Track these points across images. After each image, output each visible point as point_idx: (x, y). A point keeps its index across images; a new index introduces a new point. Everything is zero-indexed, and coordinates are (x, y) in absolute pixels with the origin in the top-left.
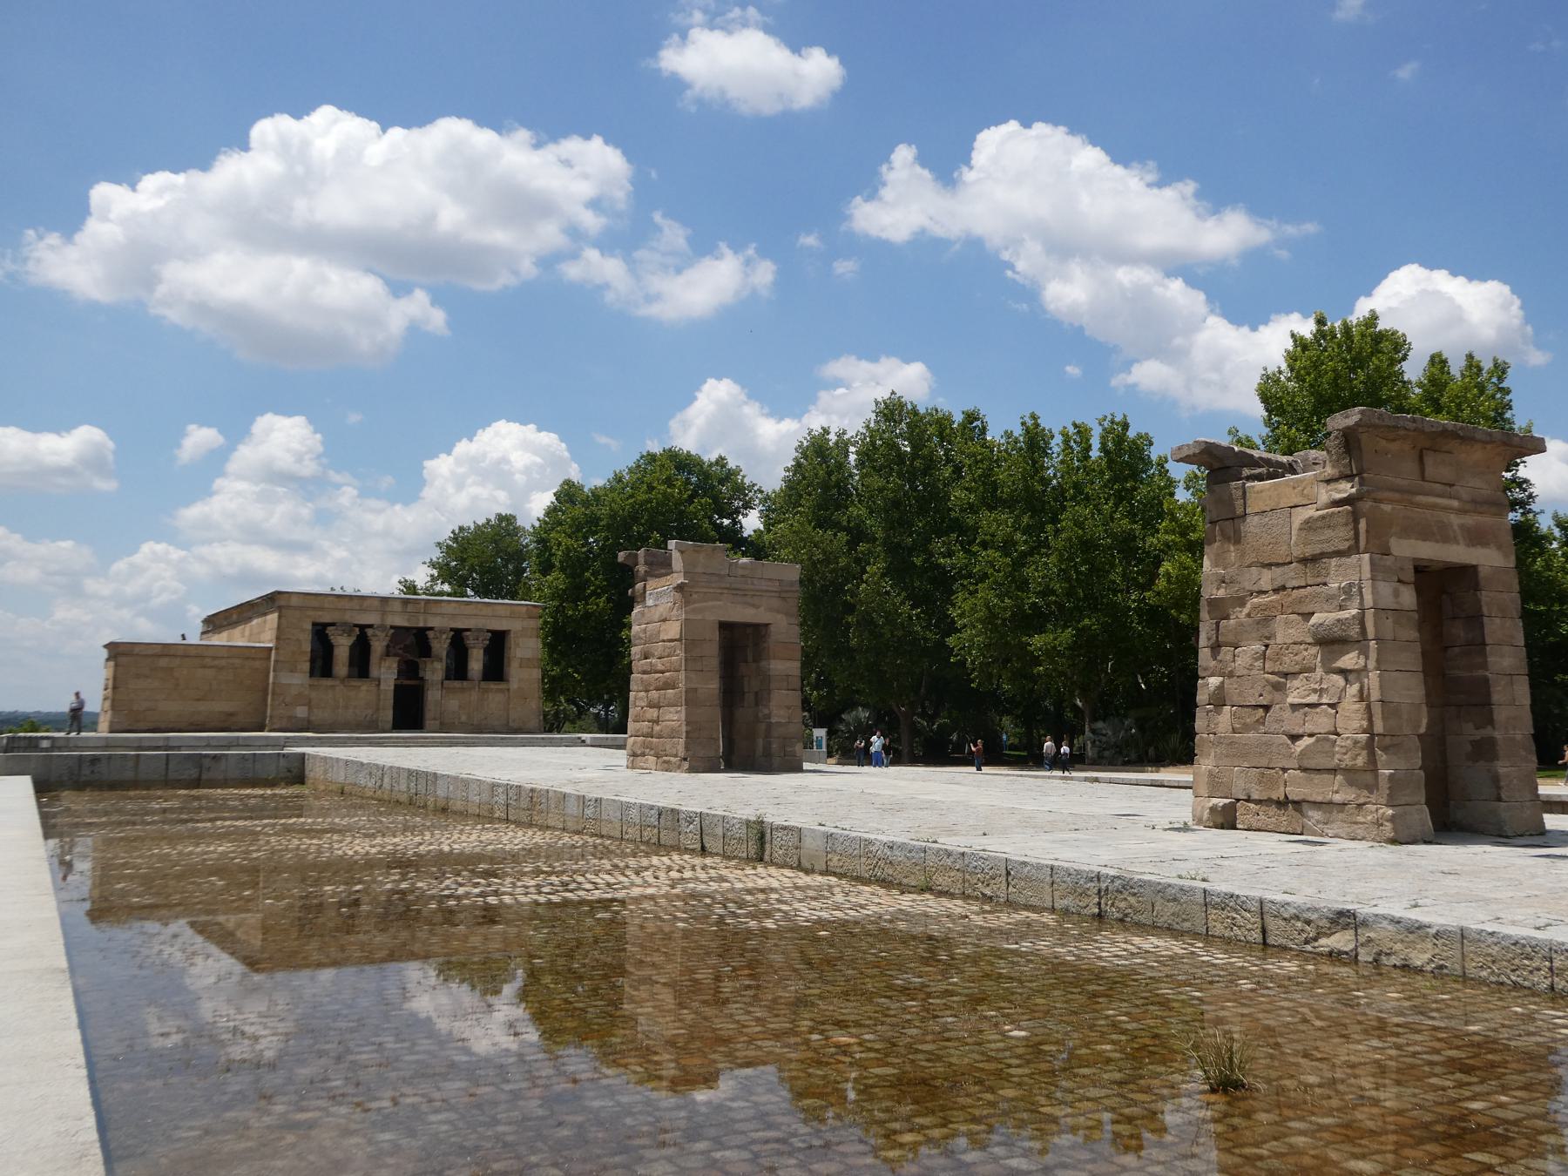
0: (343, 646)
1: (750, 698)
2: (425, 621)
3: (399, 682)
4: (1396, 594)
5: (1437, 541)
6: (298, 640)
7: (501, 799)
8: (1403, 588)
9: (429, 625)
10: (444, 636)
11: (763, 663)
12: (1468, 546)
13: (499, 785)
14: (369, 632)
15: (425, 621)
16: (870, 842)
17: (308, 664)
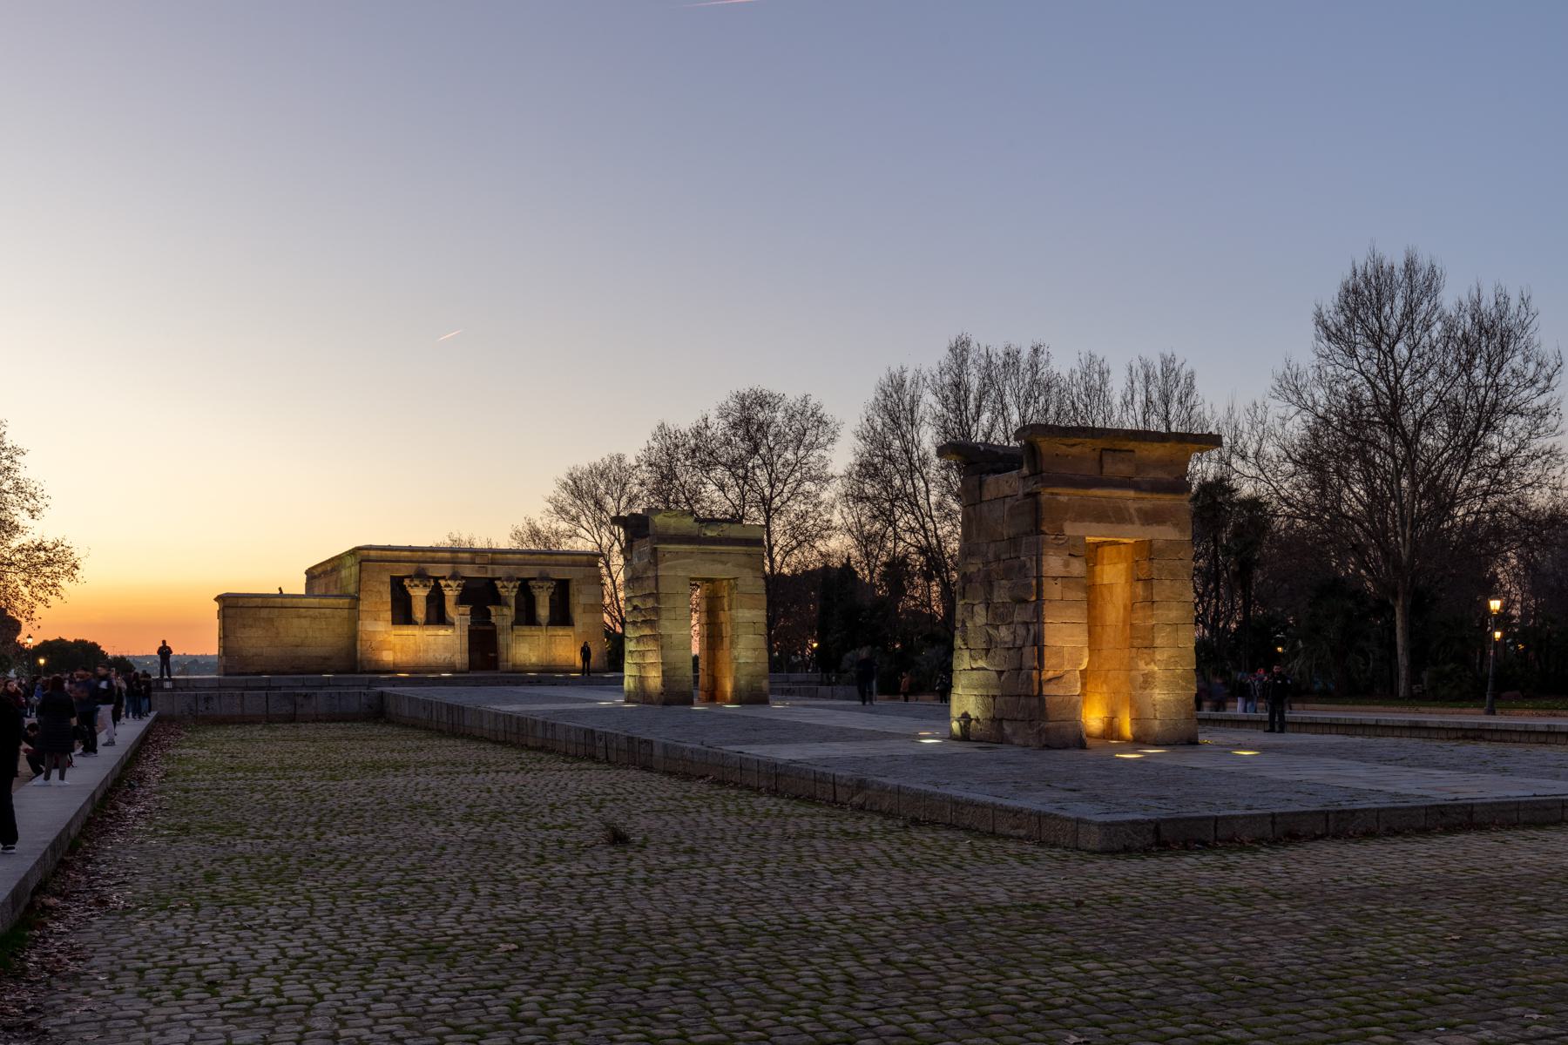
0: (419, 594)
1: (727, 641)
2: (493, 571)
3: (474, 628)
4: (1066, 565)
5: (1112, 522)
6: (379, 592)
7: (501, 726)
8: (1073, 560)
9: (497, 576)
10: (511, 585)
11: (733, 611)
12: (1143, 525)
13: (500, 715)
14: (443, 583)
15: (493, 571)
16: (683, 749)
17: (390, 613)
